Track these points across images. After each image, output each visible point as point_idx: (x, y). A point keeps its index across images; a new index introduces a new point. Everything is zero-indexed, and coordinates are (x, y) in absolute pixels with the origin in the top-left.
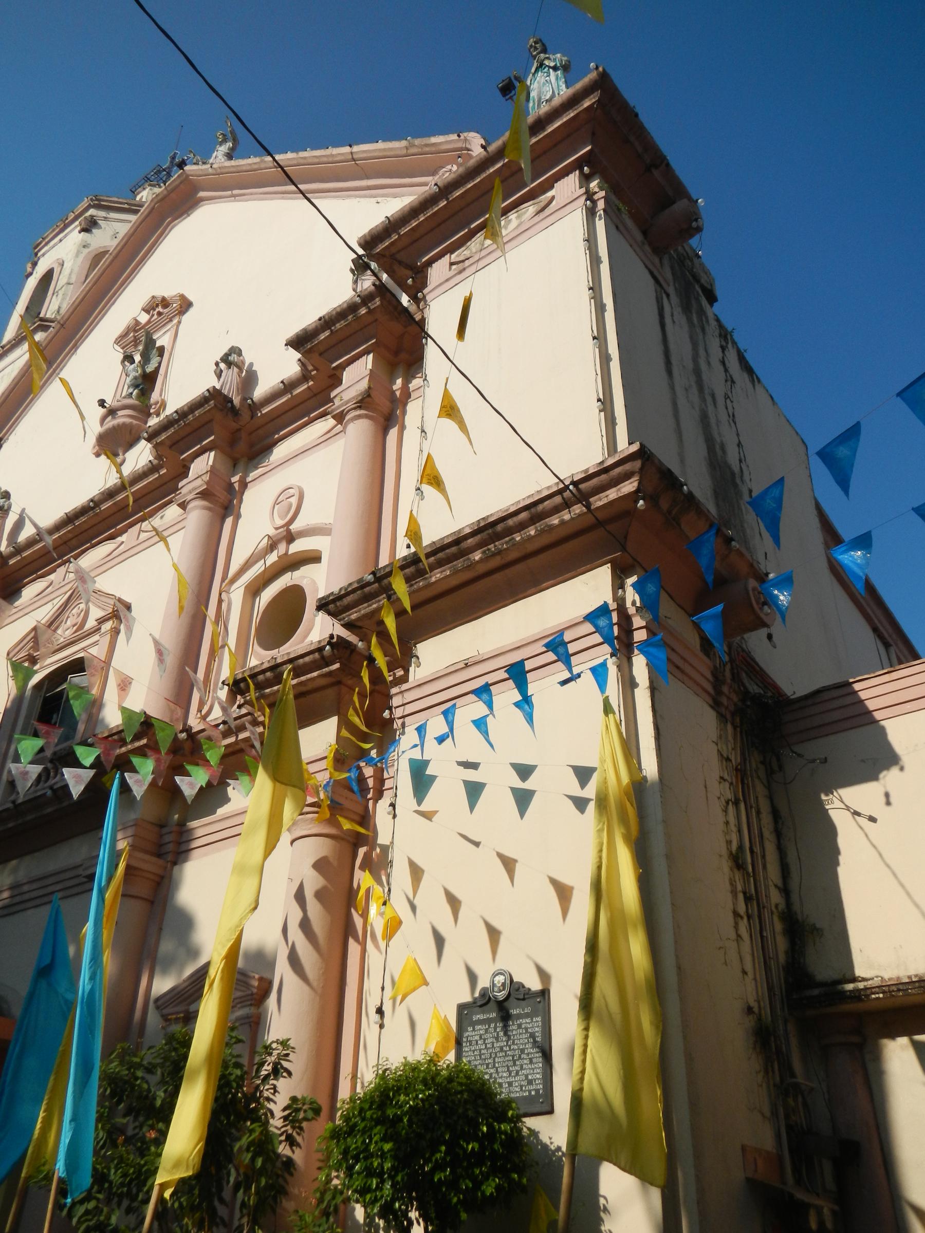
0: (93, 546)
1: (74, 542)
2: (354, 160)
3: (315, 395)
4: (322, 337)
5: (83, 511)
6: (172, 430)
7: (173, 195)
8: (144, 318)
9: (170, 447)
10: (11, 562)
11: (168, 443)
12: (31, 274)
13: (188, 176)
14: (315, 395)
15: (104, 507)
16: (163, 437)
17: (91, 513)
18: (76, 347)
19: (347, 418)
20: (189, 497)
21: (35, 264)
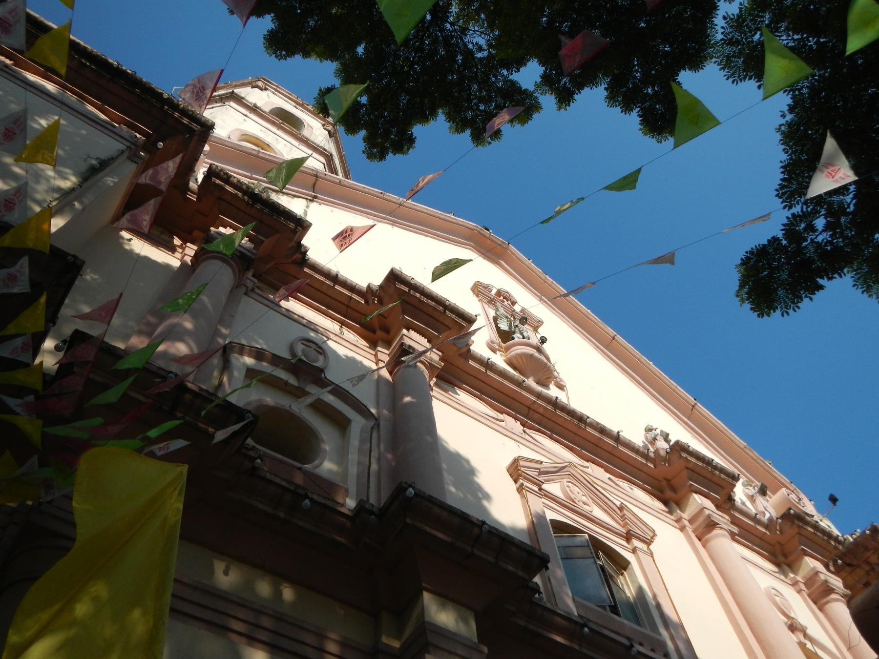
0: (551, 438)
1: (537, 416)
2: (693, 406)
3: (761, 539)
4: (810, 529)
5: (572, 413)
6: (701, 464)
7: (489, 242)
8: (494, 292)
9: (687, 468)
10: (471, 362)
11: (690, 466)
12: (261, 89)
13: (507, 249)
14: (761, 539)
15: (589, 429)
16: (693, 460)
17: (576, 422)
18: (394, 223)
19: (833, 596)
20: (723, 526)
21: (266, 89)
